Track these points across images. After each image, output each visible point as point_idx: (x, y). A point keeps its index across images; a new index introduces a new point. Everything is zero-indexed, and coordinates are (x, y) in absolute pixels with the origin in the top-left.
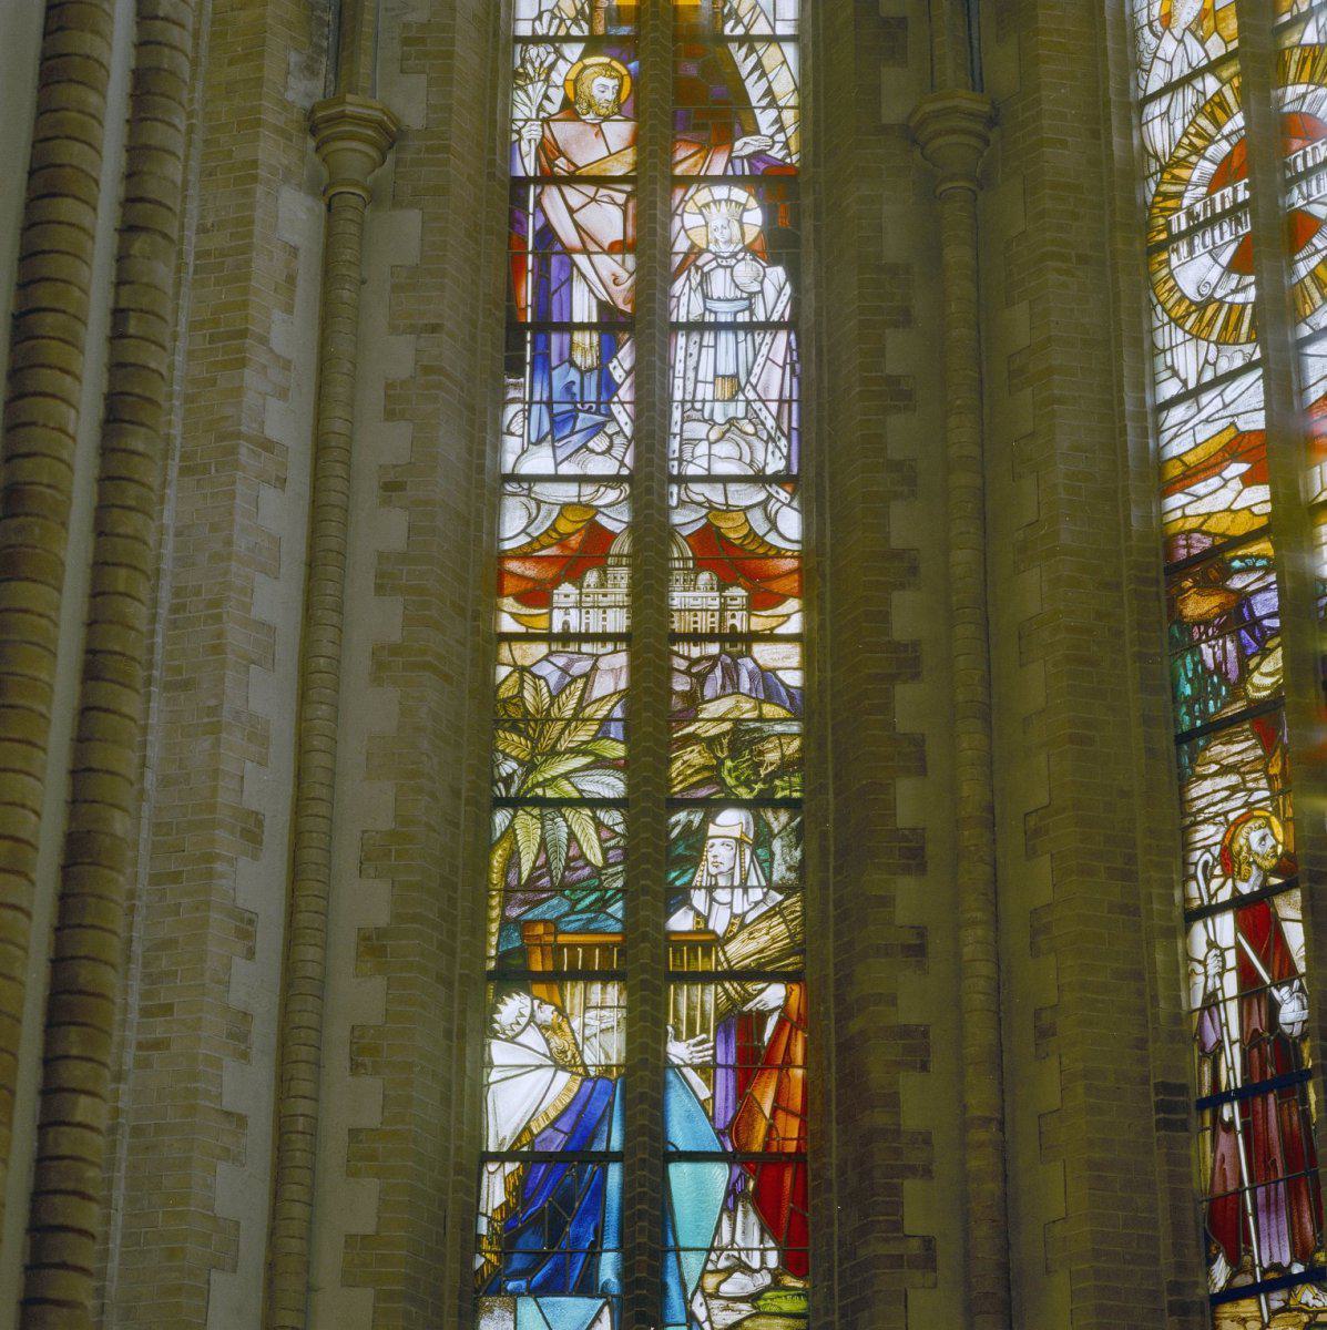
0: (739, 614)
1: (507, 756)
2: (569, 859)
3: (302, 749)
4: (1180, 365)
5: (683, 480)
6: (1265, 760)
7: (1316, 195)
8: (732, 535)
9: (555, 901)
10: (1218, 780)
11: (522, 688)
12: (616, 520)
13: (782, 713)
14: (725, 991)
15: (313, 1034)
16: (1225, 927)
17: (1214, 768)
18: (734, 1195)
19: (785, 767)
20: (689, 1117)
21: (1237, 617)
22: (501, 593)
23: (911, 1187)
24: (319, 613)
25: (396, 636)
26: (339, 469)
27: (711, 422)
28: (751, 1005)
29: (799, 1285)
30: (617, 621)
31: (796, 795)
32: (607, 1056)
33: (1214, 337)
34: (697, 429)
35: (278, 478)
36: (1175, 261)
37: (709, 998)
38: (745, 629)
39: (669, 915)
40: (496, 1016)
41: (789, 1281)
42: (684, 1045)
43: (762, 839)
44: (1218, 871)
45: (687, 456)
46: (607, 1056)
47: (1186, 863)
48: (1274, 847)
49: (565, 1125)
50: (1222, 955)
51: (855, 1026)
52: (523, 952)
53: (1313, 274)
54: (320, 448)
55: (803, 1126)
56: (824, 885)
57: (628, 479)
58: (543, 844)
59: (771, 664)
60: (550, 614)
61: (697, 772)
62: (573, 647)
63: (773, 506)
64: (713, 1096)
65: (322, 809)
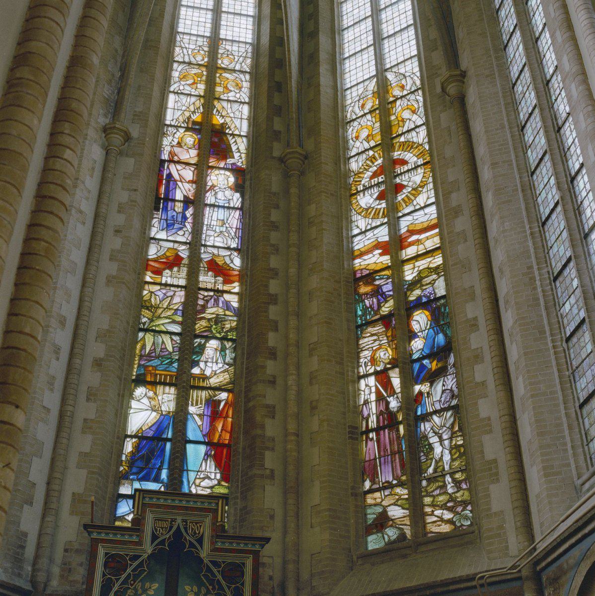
0: (220, 285)
1: (144, 317)
2: (161, 349)
3: (81, 301)
4: (360, 225)
5: (205, 246)
6: (386, 332)
7: (404, 179)
8: (219, 263)
9: (156, 361)
10: (370, 338)
11: (151, 298)
12: (184, 252)
13: (231, 314)
14: (209, 393)
15: (76, 386)
16: (372, 381)
17: (369, 334)
18: (207, 455)
19: (231, 329)
20: (194, 430)
21: (378, 292)
22: (147, 270)
23: (268, 454)
24: (91, 262)
25: (114, 273)
26: (102, 222)
27: (215, 231)
28: (216, 398)
29: (227, 485)
30: (182, 282)
31: (234, 338)
32: (169, 409)
33: (371, 217)
34: (210, 233)
35: (83, 222)
36: (358, 197)
37: (204, 394)
38: (222, 289)
39: (192, 368)
40: (134, 393)
41: (223, 483)
42: (194, 408)
43: (223, 349)
44: (369, 364)
45: (207, 239)
46: (169, 409)
47: (358, 362)
48: (389, 356)
49: (154, 428)
50: (370, 388)
51: (251, 404)
52: (144, 375)
53: (403, 199)
54: (97, 216)
55: (230, 437)
56: (242, 363)
57: (189, 244)
58: (154, 343)
59: (229, 300)
60: (162, 278)
61: (204, 328)
62: (168, 288)
63: (232, 257)
64: (202, 424)
65: (86, 318)
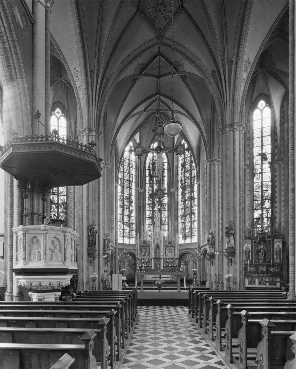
37: (266, 210)
43: (269, 201)
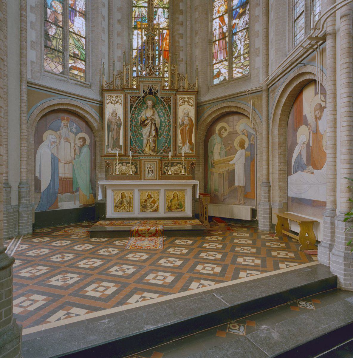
16: (218, 20)
23: (181, 52)
43: (164, 12)
47: (213, 13)
51: (174, 34)
56: (171, 18)
58: (139, 12)
